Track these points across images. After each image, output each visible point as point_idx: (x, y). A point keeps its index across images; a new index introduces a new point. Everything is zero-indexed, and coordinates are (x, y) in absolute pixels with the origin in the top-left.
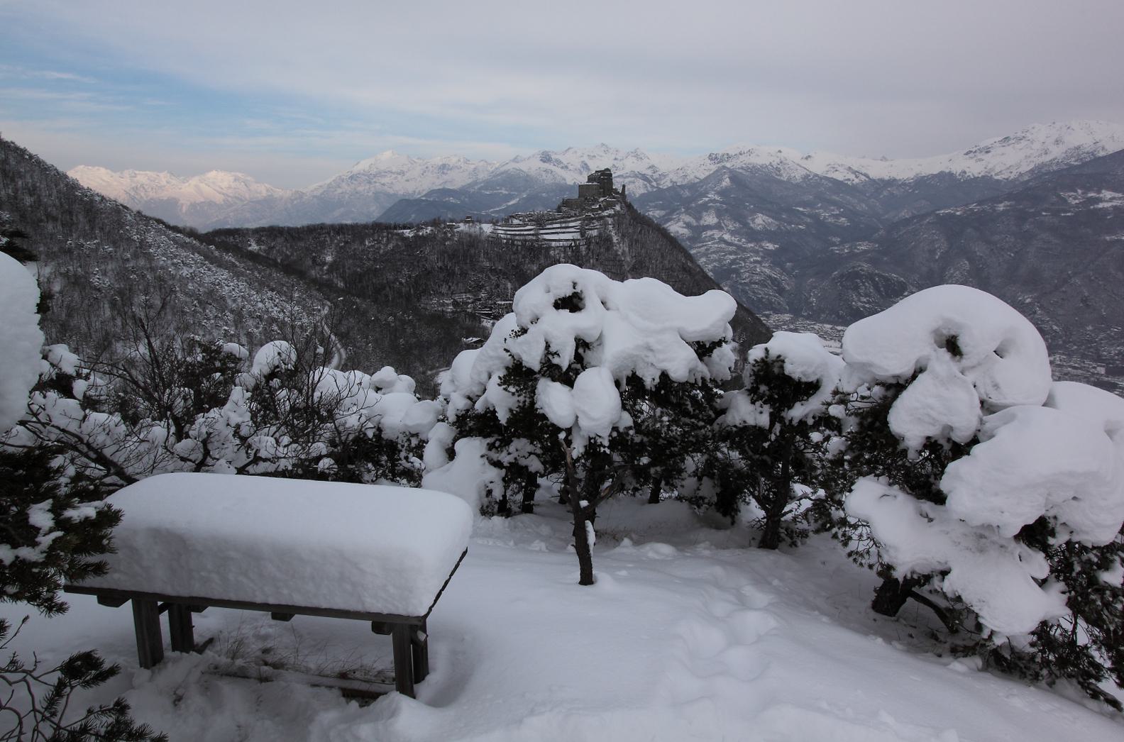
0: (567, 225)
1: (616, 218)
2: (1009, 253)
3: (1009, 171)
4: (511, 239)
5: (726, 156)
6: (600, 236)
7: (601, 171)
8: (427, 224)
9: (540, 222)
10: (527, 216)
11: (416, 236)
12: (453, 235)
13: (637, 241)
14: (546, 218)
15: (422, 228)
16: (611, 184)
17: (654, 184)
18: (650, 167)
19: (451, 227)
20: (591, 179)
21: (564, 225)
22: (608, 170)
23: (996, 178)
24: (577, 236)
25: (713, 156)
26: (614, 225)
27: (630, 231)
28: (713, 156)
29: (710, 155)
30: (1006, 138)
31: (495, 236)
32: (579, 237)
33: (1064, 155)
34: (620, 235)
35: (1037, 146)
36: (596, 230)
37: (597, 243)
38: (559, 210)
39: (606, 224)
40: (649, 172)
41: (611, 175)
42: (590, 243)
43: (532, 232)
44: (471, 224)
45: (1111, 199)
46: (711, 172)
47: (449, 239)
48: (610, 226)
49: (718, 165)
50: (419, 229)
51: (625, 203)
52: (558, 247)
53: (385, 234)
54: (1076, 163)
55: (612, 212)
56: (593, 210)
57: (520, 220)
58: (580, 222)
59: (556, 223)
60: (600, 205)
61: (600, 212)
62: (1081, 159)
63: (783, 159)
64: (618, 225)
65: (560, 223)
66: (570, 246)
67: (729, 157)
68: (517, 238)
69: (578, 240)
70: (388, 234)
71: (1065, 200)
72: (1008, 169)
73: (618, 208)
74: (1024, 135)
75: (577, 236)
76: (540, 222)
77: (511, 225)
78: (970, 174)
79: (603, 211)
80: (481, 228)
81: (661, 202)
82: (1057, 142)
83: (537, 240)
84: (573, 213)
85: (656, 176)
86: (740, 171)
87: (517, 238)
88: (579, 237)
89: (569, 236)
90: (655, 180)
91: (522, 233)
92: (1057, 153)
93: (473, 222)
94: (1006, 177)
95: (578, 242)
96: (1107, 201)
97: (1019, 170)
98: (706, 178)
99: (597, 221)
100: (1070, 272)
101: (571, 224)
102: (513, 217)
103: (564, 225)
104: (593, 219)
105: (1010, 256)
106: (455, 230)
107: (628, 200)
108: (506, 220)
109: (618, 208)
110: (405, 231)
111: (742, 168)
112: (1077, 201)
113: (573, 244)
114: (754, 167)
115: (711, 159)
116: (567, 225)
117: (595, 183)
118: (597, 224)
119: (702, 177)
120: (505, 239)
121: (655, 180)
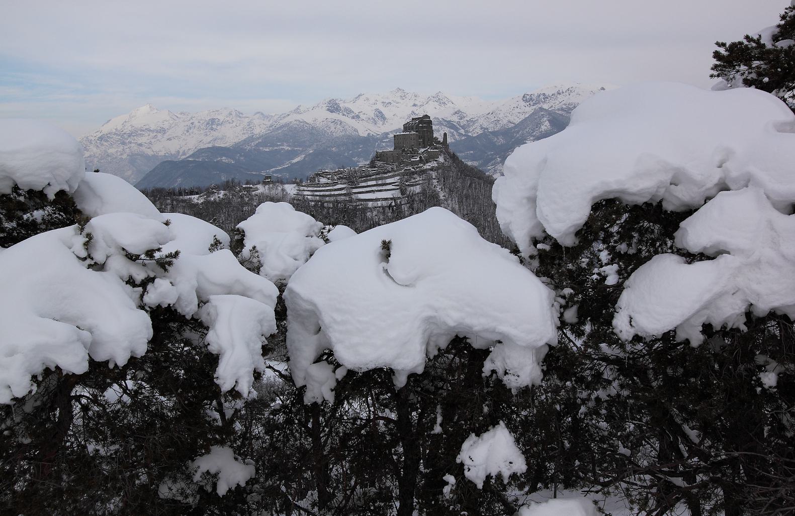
0: (383, 181)
1: (440, 171)
4: (320, 201)
5: (542, 97)
6: (424, 192)
7: (418, 118)
8: (218, 188)
9: (352, 180)
10: (336, 173)
11: (207, 203)
12: (251, 199)
13: (467, 197)
14: (359, 174)
15: (213, 193)
16: (432, 132)
17: (462, 131)
18: (456, 113)
19: (248, 190)
20: (407, 127)
21: (380, 182)
22: (426, 116)
24: (397, 193)
25: (528, 97)
26: (439, 179)
27: (459, 184)
28: (528, 97)
29: (524, 97)
31: (301, 198)
32: (400, 195)
34: (447, 190)
36: (418, 186)
37: (421, 201)
38: (372, 165)
39: (430, 179)
40: (455, 119)
42: (413, 201)
43: (343, 192)
44: (271, 185)
46: (527, 116)
47: (247, 204)
48: (434, 181)
49: (534, 107)
50: (209, 192)
51: (449, 154)
52: (375, 207)
53: (169, 201)
55: (434, 164)
56: (412, 164)
58: (398, 178)
59: (373, 180)
60: (420, 157)
61: (421, 165)
64: (443, 179)
65: (376, 179)
66: (390, 206)
67: (546, 97)
68: (327, 199)
69: (399, 198)
70: (172, 201)
73: (441, 159)
75: (397, 193)
76: (352, 180)
77: (318, 185)
79: (424, 164)
80: (283, 190)
81: (472, 152)
83: (351, 201)
84: (389, 167)
85: (463, 122)
86: (560, 112)
87: (327, 199)
88: (400, 195)
89: (388, 195)
90: (463, 127)
91: (333, 193)
93: (272, 182)
95: (398, 201)
98: (522, 122)
99: (420, 175)
101: (388, 181)
102: (319, 175)
103: (380, 182)
104: (413, 173)
106: (253, 193)
107: (452, 149)
108: (312, 179)
109: (441, 159)
110: (193, 196)
111: (562, 109)
113: (393, 204)
115: (526, 101)
116: (383, 181)
117: (413, 133)
118: (418, 179)
119: (517, 121)
120: (312, 201)
121: (463, 127)
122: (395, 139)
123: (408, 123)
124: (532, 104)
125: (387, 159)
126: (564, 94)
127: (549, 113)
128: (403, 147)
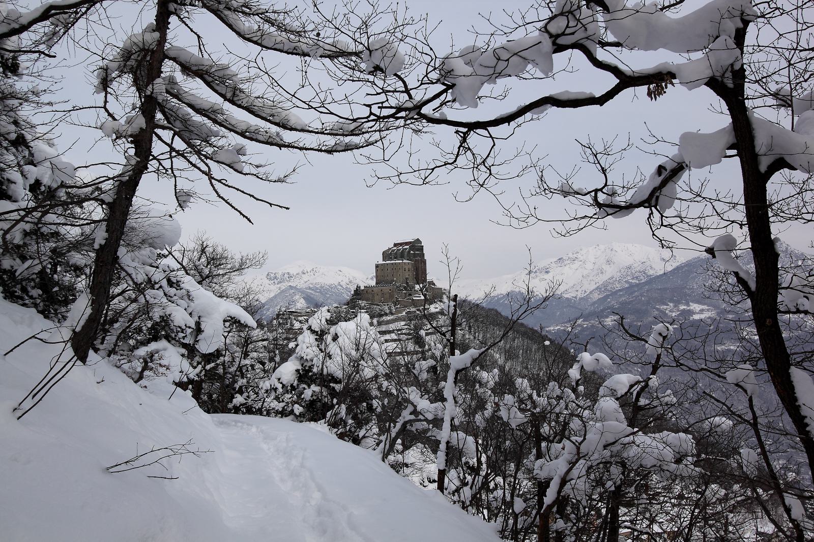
2: (636, 368)
3: (574, 289)
5: (286, 276)
7: (406, 244)
22: (418, 241)
23: (566, 296)
25: (272, 275)
28: (272, 275)
30: (560, 259)
33: (619, 274)
35: (589, 266)
41: (421, 249)
45: (702, 311)
46: (272, 295)
54: (633, 281)
57: (301, 322)
58: (403, 323)
62: (637, 277)
63: (351, 279)
71: (663, 312)
72: (573, 287)
74: (575, 256)
78: (538, 293)
82: (609, 262)
92: (610, 272)
94: (574, 295)
96: (698, 313)
97: (583, 288)
100: (701, 385)
101: (392, 327)
105: (638, 371)
111: (310, 288)
112: (674, 314)
114: (322, 287)
115: (270, 279)
117: (405, 261)
122: (377, 271)
123: (389, 249)
124: (276, 283)
125: (373, 296)
126: (309, 273)
127: (301, 291)
128: (393, 281)
